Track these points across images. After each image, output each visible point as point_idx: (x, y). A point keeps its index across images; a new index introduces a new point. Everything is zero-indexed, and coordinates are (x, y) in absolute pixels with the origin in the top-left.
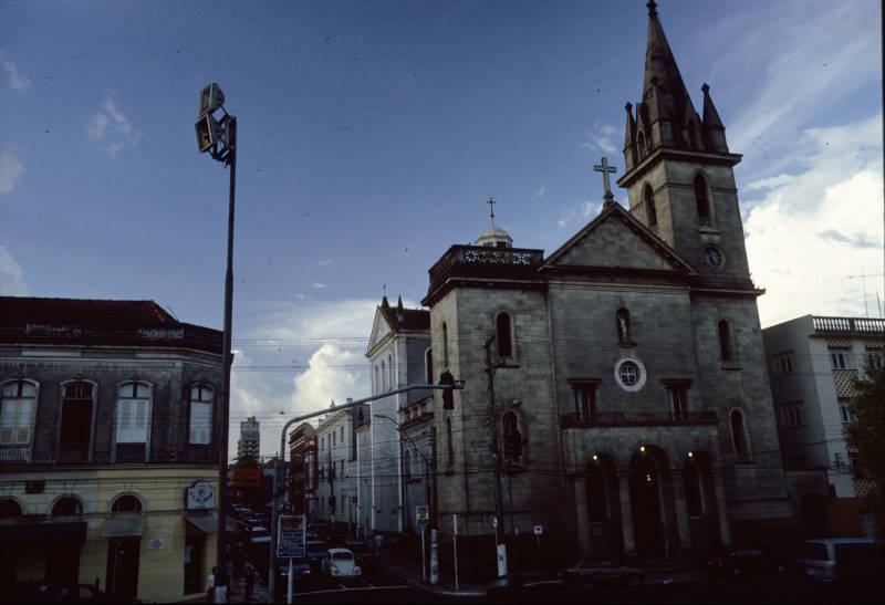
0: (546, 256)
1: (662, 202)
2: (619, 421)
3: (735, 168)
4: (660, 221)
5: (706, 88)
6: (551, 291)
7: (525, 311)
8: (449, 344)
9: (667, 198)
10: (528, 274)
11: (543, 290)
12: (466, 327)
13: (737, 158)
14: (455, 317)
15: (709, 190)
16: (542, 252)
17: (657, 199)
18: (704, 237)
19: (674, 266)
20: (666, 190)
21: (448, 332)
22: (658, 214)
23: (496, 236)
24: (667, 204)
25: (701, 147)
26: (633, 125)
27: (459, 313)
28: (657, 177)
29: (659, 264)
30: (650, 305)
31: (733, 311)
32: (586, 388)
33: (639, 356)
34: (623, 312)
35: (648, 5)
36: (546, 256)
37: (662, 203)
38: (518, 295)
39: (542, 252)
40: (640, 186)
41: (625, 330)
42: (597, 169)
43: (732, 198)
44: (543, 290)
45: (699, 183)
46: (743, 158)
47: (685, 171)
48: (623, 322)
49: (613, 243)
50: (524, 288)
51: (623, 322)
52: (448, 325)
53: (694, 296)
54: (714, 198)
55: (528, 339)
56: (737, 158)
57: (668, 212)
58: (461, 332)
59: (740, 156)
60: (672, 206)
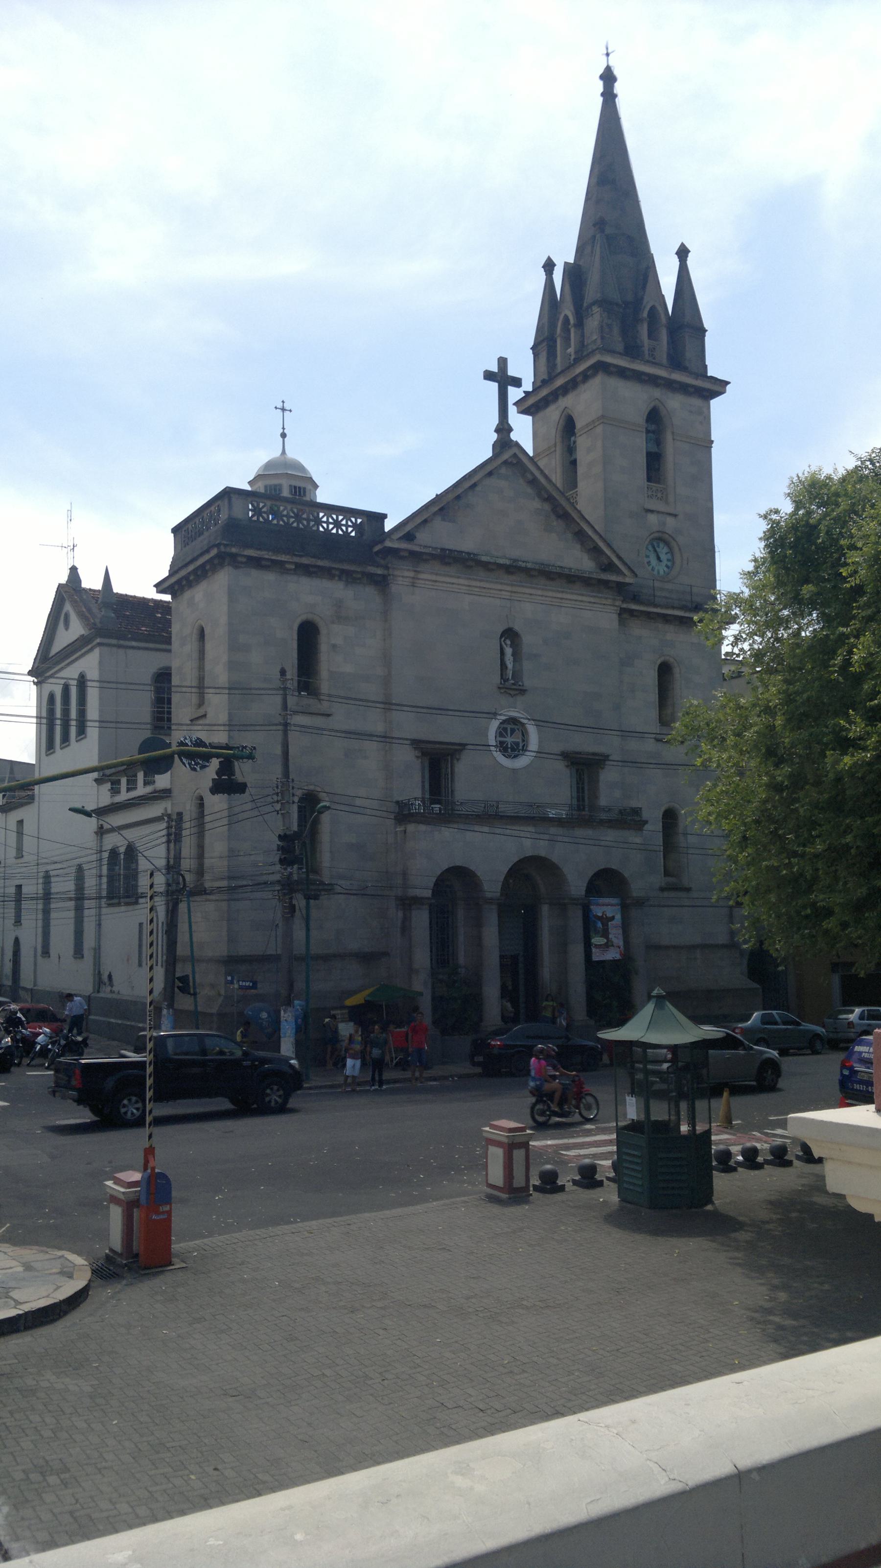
0: (389, 525)
1: (588, 450)
2: (490, 816)
4: (582, 485)
5: (683, 253)
6: (394, 588)
7: (340, 617)
8: (208, 666)
10: (366, 551)
11: (382, 583)
13: (719, 387)
14: (223, 620)
15: (669, 437)
16: (381, 518)
17: (582, 442)
18: (653, 518)
20: (599, 430)
21: (208, 646)
22: (581, 470)
25: (664, 358)
28: (585, 403)
29: (579, 560)
31: (678, 644)
32: (438, 761)
34: (510, 635)
35: (602, 77)
36: (389, 525)
38: (337, 589)
40: (554, 413)
41: (510, 665)
42: (489, 376)
44: (382, 583)
45: (655, 419)
46: (728, 387)
47: (634, 400)
48: (509, 651)
50: (348, 577)
51: (509, 651)
52: (207, 631)
53: (625, 615)
55: (348, 669)
56: (719, 387)
58: (234, 646)
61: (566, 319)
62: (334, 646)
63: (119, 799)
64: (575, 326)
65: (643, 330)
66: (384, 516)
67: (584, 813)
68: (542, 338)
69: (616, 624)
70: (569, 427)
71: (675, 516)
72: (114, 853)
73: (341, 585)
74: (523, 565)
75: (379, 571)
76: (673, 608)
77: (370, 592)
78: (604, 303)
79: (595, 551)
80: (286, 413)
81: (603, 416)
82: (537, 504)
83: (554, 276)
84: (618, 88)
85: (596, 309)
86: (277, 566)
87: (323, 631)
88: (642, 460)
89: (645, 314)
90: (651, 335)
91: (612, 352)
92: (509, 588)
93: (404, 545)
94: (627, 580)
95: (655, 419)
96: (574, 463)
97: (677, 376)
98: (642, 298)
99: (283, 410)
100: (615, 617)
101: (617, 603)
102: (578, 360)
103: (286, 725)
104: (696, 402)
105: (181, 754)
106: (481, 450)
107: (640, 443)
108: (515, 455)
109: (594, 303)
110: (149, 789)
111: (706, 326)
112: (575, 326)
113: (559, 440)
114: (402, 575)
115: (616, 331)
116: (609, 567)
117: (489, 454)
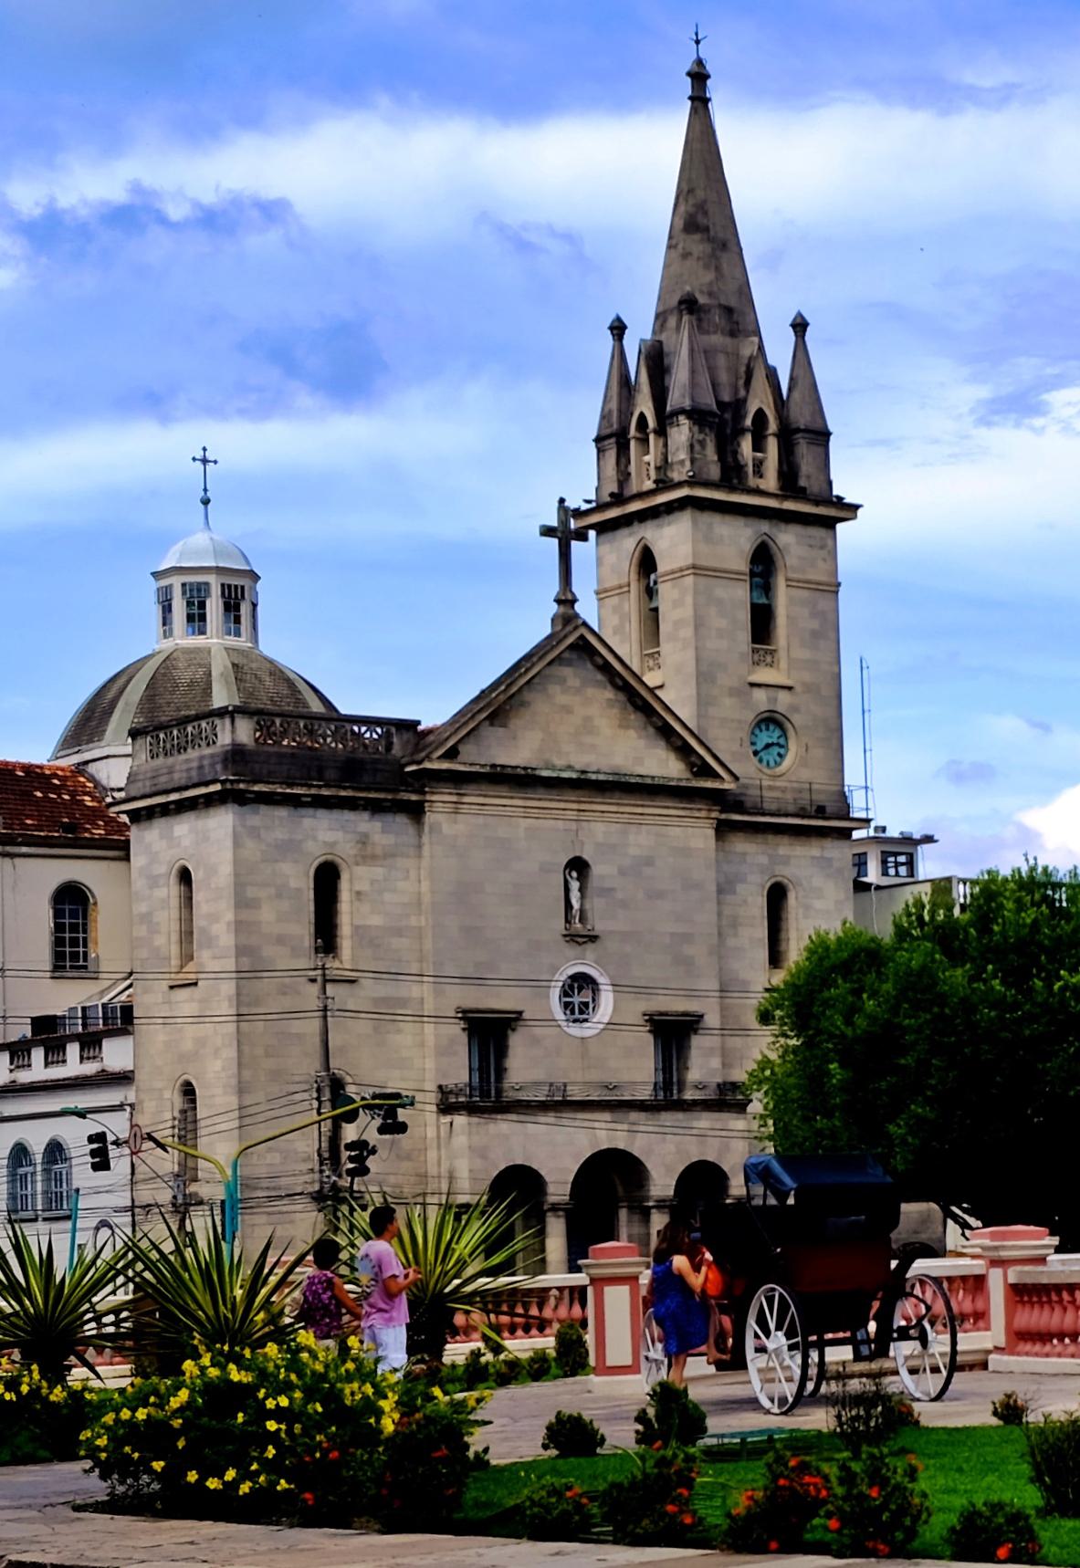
1: (675, 601)
3: (839, 526)
4: (665, 647)
5: (800, 326)
6: (429, 818)
7: (367, 858)
8: (198, 922)
9: (689, 600)
11: (416, 812)
12: (251, 892)
17: (666, 594)
18: (760, 696)
19: (690, 766)
21: (198, 896)
23: (219, 570)
24: (687, 612)
26: (625, 387)
27: (236, 862)
28: (674, 541)
29: (663, 765)
30: (633, 851)
33: (598, 962)
37: (677, 604)
38: (363, 822)
39: (418, 723)
40: (627, 542)
42: (547, 531)
43: (823, 603)
46: (860, 512)
47: (734, 541)
49: (568, 710)
50: (376, 808)
53: (724, 830)
54: (791, 601)
55: (376, 920)
57: (688, 632)
58: (242, 902)
59: (857, 507)
60: (699, 623)
61: (642, 417)
62: (358, 893)
63: (24, 1077)
64: (655, 432)
65: (746, 445)
66: (418, 723)
67: (669, 1097)
68: (608, 431)
69: (712, 841)
70: (647, 562)
71: (790, 688)
72: (20, 1154)
73: (366, 815)
74: (594, 777)
75: (414, 797)
76: (786, 815)
77: (401, 820)
78: (697, 416)
79: (684, 751)
80: (210, 466)
81: (694, 567)
82: (609, 694)
83: (625, 342)
84: (714, 89)
85: (682, 419)
86: (294, 802)
87: (345, 877)
88: (745, 616)
89: (748, 422)
90: (758, 446)
91: (707, 484)
92: (575, 806)
93: (445, 765)
94: (726, 786)
95: (763, 563)
96: (656, 610)
97: (789, 505)
98: (745, 401)
99: (205, 461)
100: (711, 833)
101: (714, 815)
102: (663, 484)
103: (325, 1009)
104: (818, 532)
105: (364, 1107)
106: (536, 626)
107: (740, 595)
108: (582, 637)
109: (682, 411)
110: (90, 1068)
111: (831, 427)
112: (655, 432)
113: (634, 576)
114: (440, 802)
115: (711, 453)
116: (704, 770)
117: (546, 630)
